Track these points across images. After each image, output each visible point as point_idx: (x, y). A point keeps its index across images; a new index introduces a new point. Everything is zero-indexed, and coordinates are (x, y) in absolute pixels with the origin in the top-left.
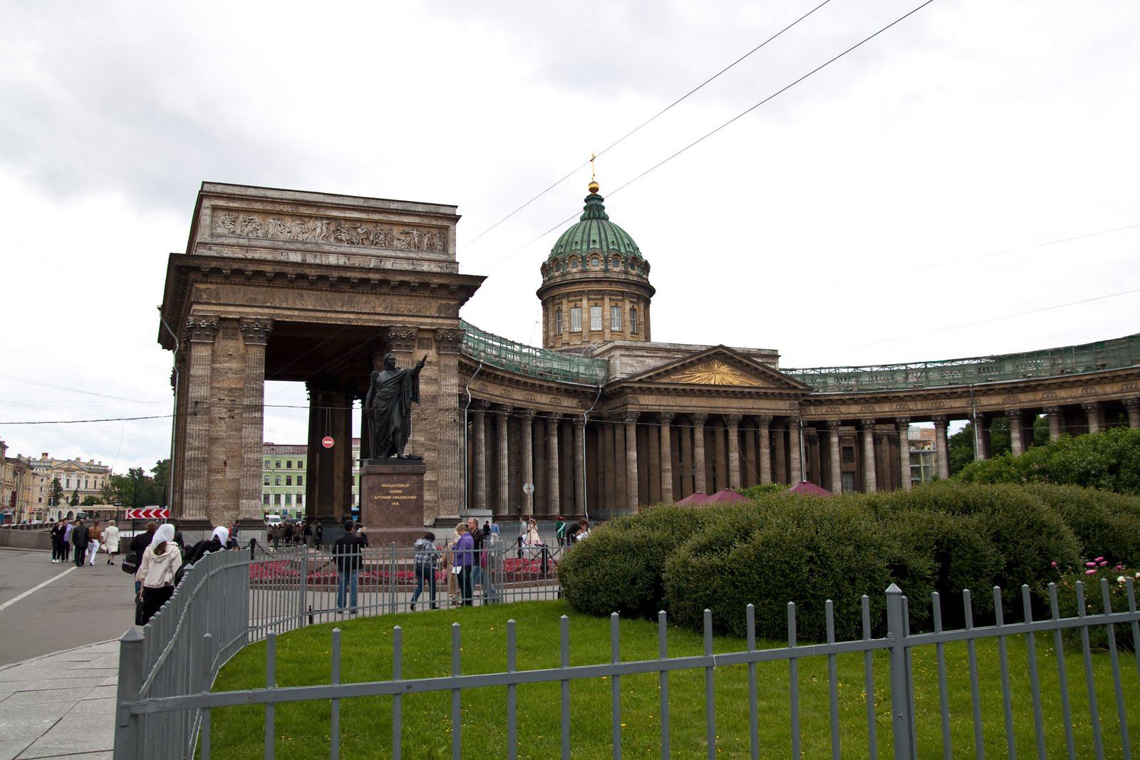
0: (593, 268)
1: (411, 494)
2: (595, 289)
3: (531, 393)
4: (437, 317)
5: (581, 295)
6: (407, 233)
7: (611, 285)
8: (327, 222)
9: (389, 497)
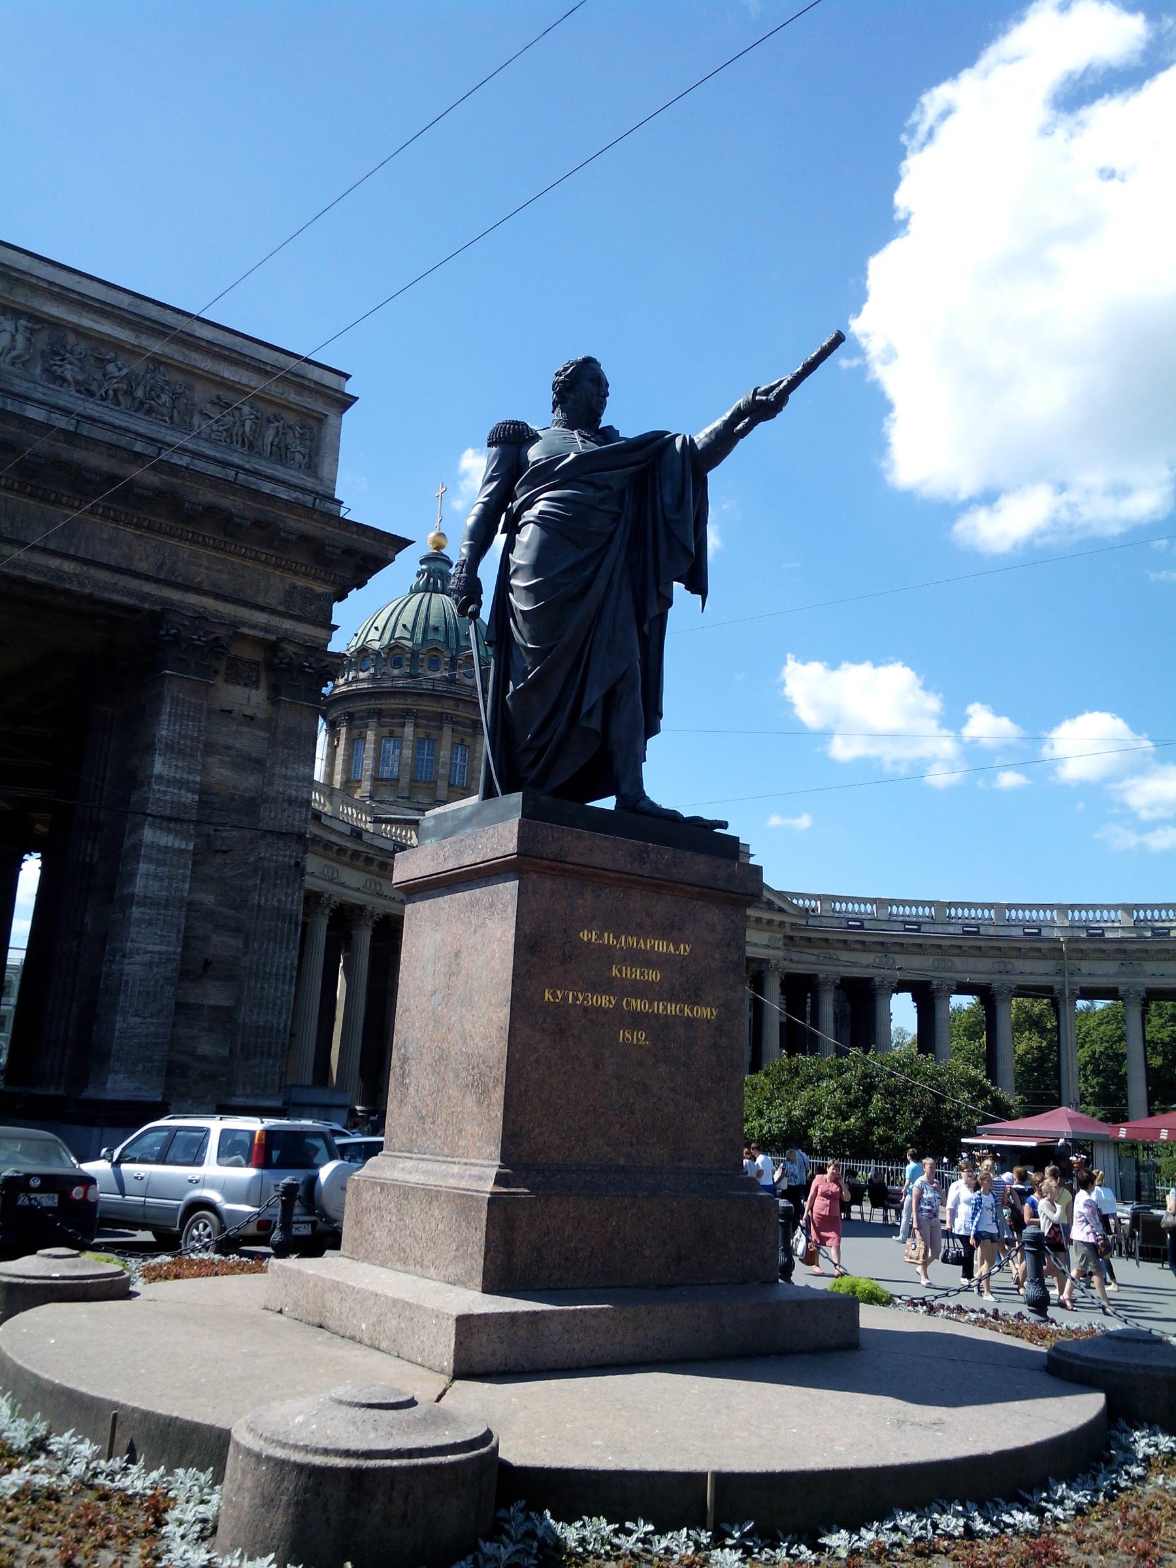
1: (695, 998)
3: (335, 865)
4: (281, 614)
5: (404, 717)
6: (228, 405)
7: (457, 705)
8: (30, 325)
9: (604, 1001)
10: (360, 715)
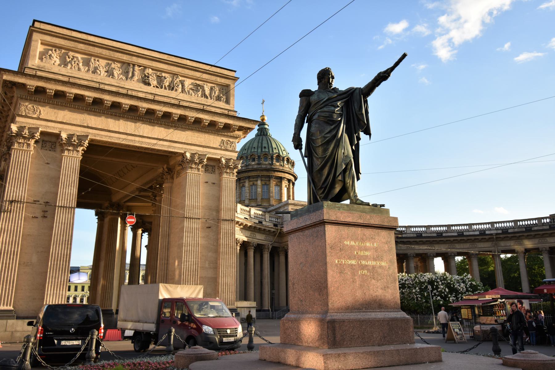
0: (264, 163)
2: (265, 174)
5: (257, 178)
9: (353, 262)
10: (242, 178)
